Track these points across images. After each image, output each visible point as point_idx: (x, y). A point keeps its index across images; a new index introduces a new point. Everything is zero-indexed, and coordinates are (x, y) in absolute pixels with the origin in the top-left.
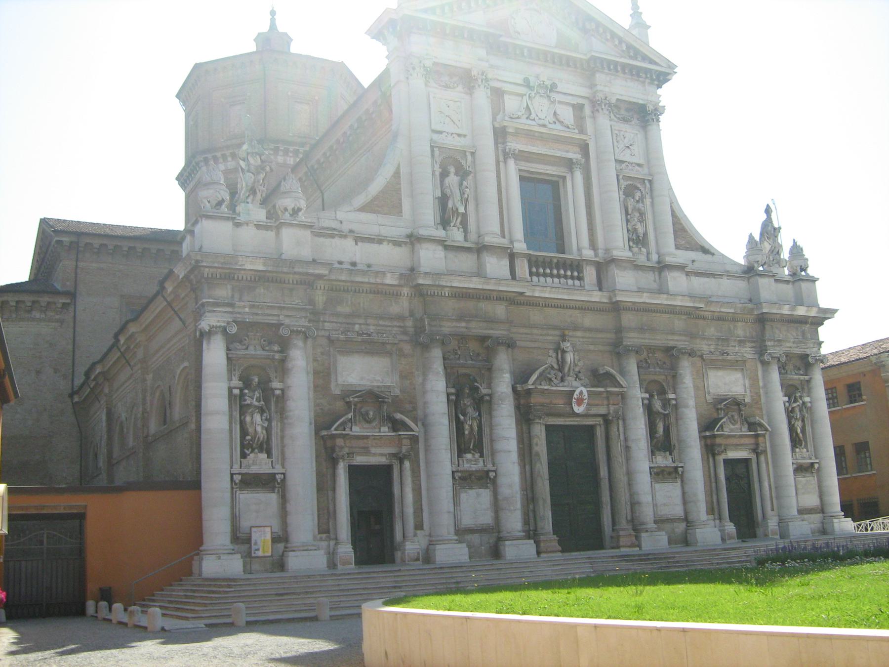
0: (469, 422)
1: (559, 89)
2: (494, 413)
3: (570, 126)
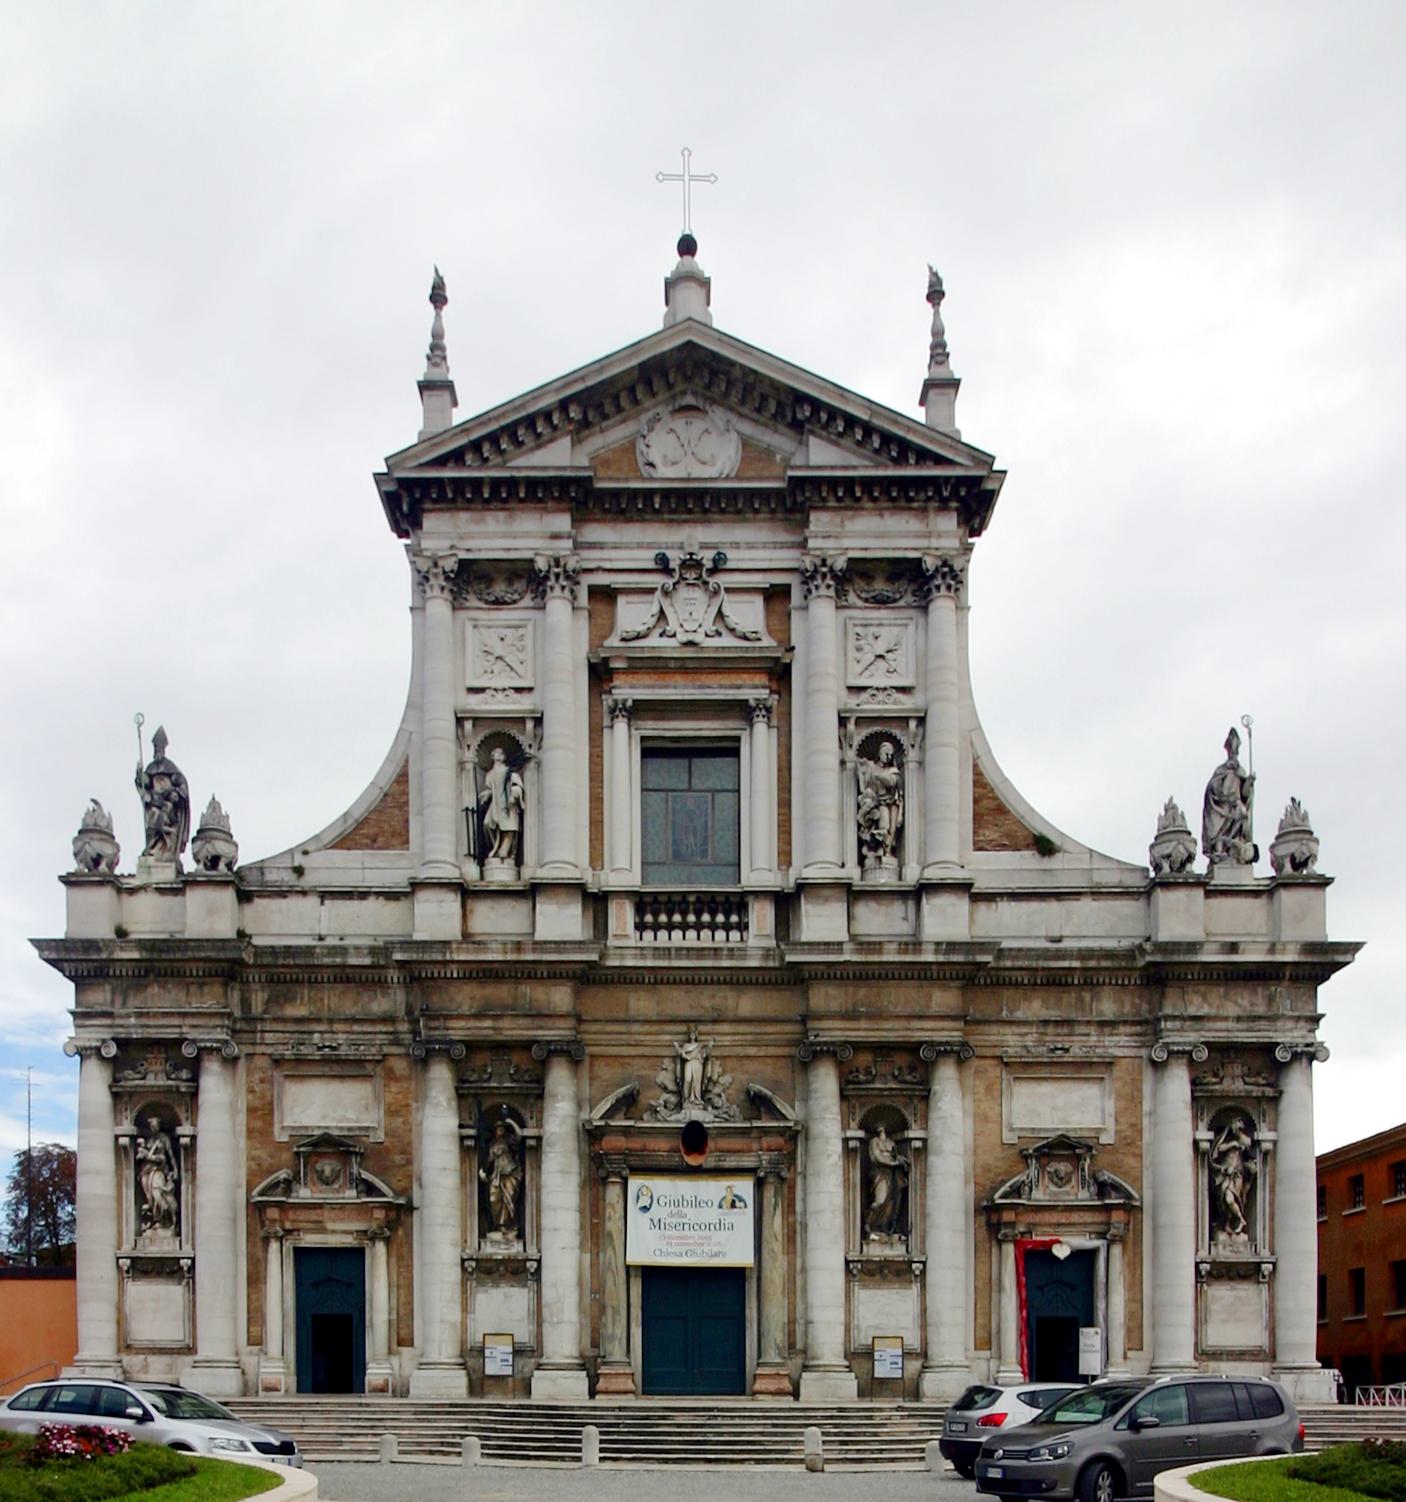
0: (496, 1182)
1: (730, 565)
2: (543, 1166)
3: (748, 635)
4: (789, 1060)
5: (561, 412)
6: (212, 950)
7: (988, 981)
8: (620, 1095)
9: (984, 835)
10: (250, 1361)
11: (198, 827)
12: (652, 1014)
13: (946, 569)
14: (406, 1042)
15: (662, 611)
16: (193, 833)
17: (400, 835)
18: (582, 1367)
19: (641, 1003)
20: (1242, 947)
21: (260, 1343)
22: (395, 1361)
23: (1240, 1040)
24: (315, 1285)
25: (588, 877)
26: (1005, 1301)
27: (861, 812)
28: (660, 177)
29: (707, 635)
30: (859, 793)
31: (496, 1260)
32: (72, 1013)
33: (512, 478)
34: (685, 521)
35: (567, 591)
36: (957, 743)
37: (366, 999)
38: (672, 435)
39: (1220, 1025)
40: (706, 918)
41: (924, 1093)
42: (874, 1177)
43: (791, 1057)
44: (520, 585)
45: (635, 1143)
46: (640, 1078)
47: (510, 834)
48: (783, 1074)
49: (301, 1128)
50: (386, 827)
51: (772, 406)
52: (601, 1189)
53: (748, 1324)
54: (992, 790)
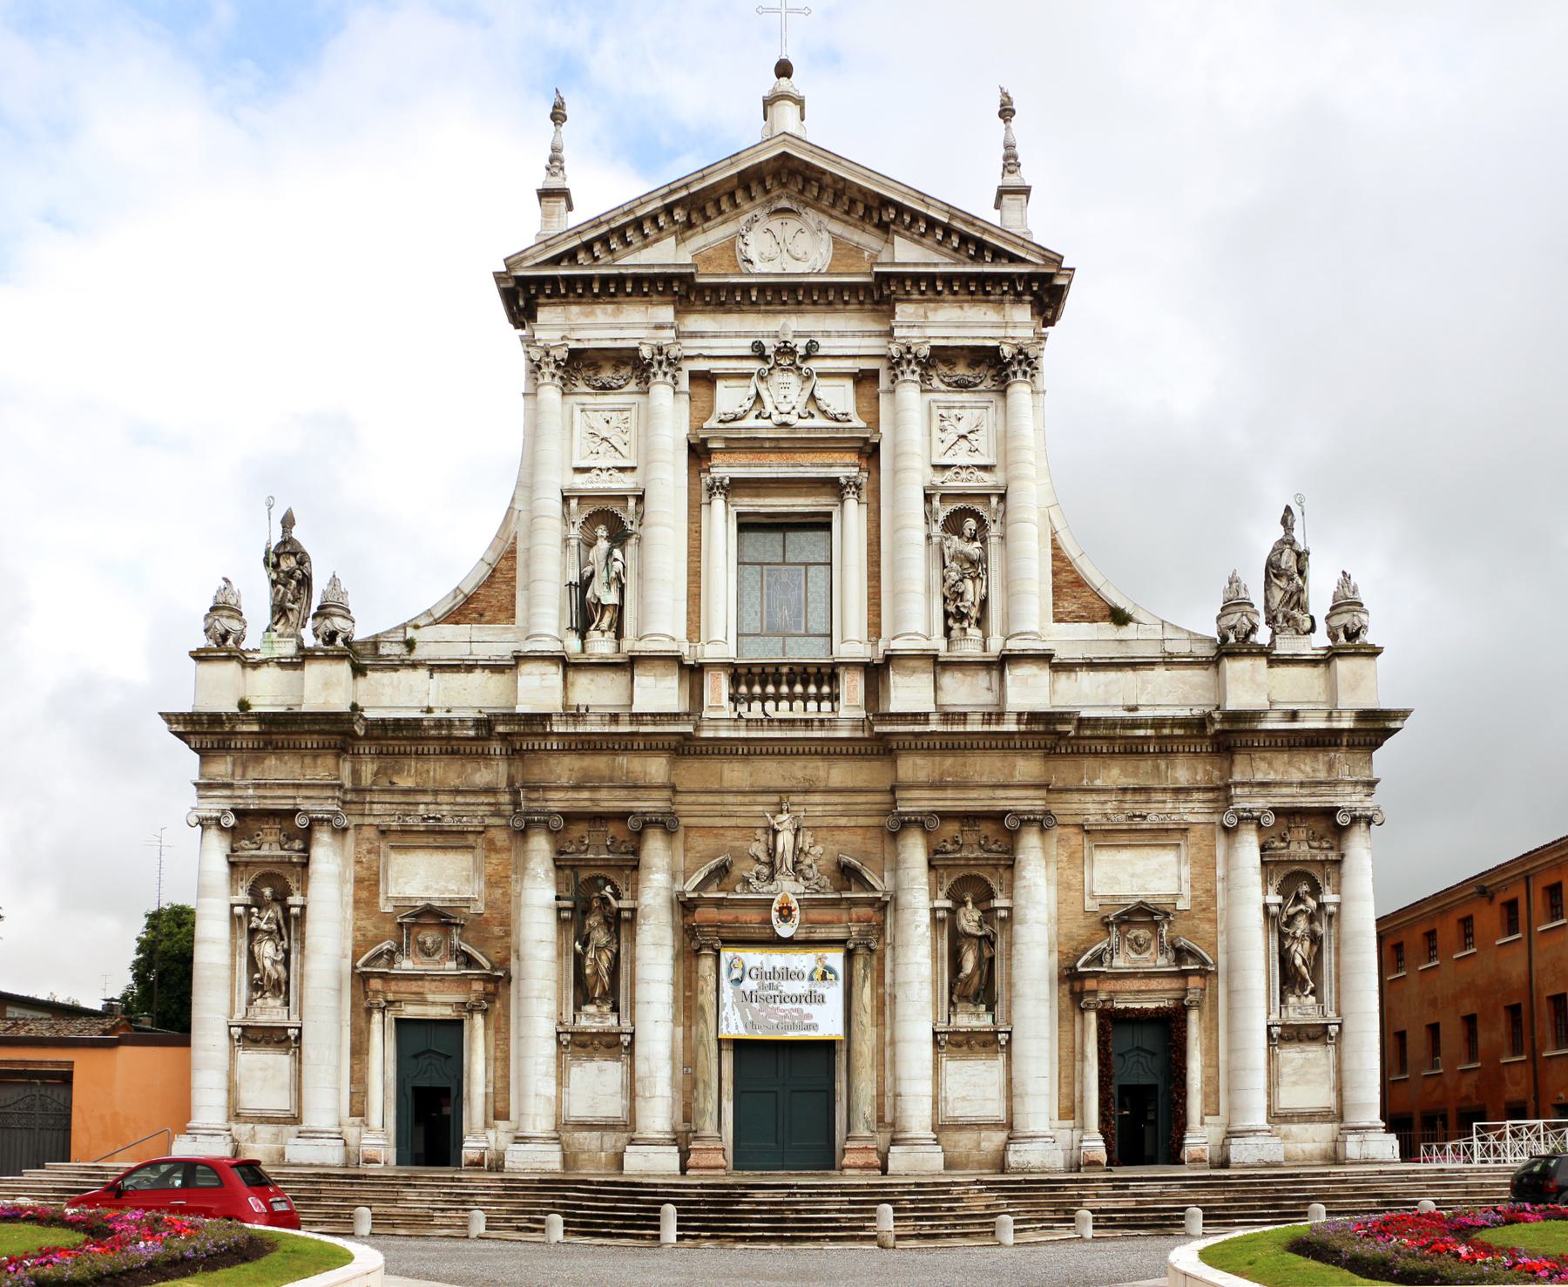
0: (591, 955)
1: (821, 353)
3: (839, 416)
4: (878, 830)
5: (666, 216)
6: (326, 723)
7: (1069, 750)
9: (1064, 607)
10: (351, 1133)
11: (318, 604)
13: (1021, 357)
14: (507, 813)
15: (758, 394)
16: (314, 610)
17: (507, 609)
18: (674, 1142)
19: (735, 773)
20: (1302, 715)
21: (362, 1115)
22: (491, 1134)
23: (1304, 805)
24: (415, 1056)
25: (685, 649)
26: (1087, 1069)
27: (947, 585)
28: (760, 10)
29: (800, 417)
30: (945, 567)
31: (591, 1033)
32: (195, 784)
33: (621, 275)
34: (780, 312)
35: (669, 378)
36: (1036, 519)
37: (469, 770)
38: (769, 234)
40: (798, 689)
41: (1010, 863)
42: (961, 947)
43: (881, 827)
44: (625, 371)
45: (726, 915)
46: (733, 849)
47: (611, 609)
48: (873, 846)
50: (494, 602)
52: (694, 963)
53: (837, 1098)
54: (1070, 564)
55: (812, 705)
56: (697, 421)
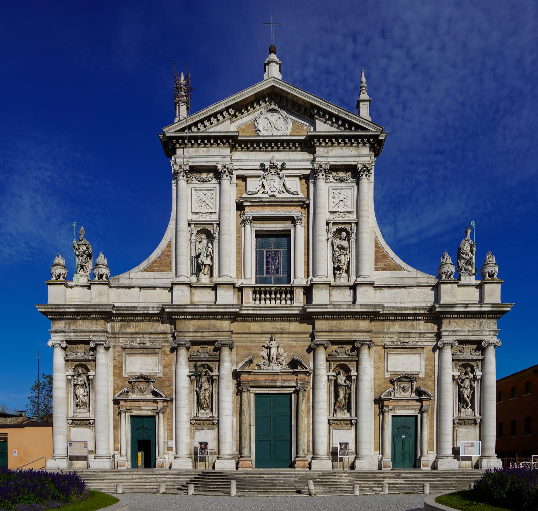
0: (202, 392)
8: (247, 360)
12: (259, 331)
14: (170, 341)
17: (168, 266)
19: (255, 326)
23: (469, 339)
29: (279, 193)
33: (209, 136)
35: (228, 177)
39: (462, 333)
46: (255, 354)
49: (132, 372)
50: (163, 263)
51: (303, 110)
55: (283, 302)
56: (239, 194)
